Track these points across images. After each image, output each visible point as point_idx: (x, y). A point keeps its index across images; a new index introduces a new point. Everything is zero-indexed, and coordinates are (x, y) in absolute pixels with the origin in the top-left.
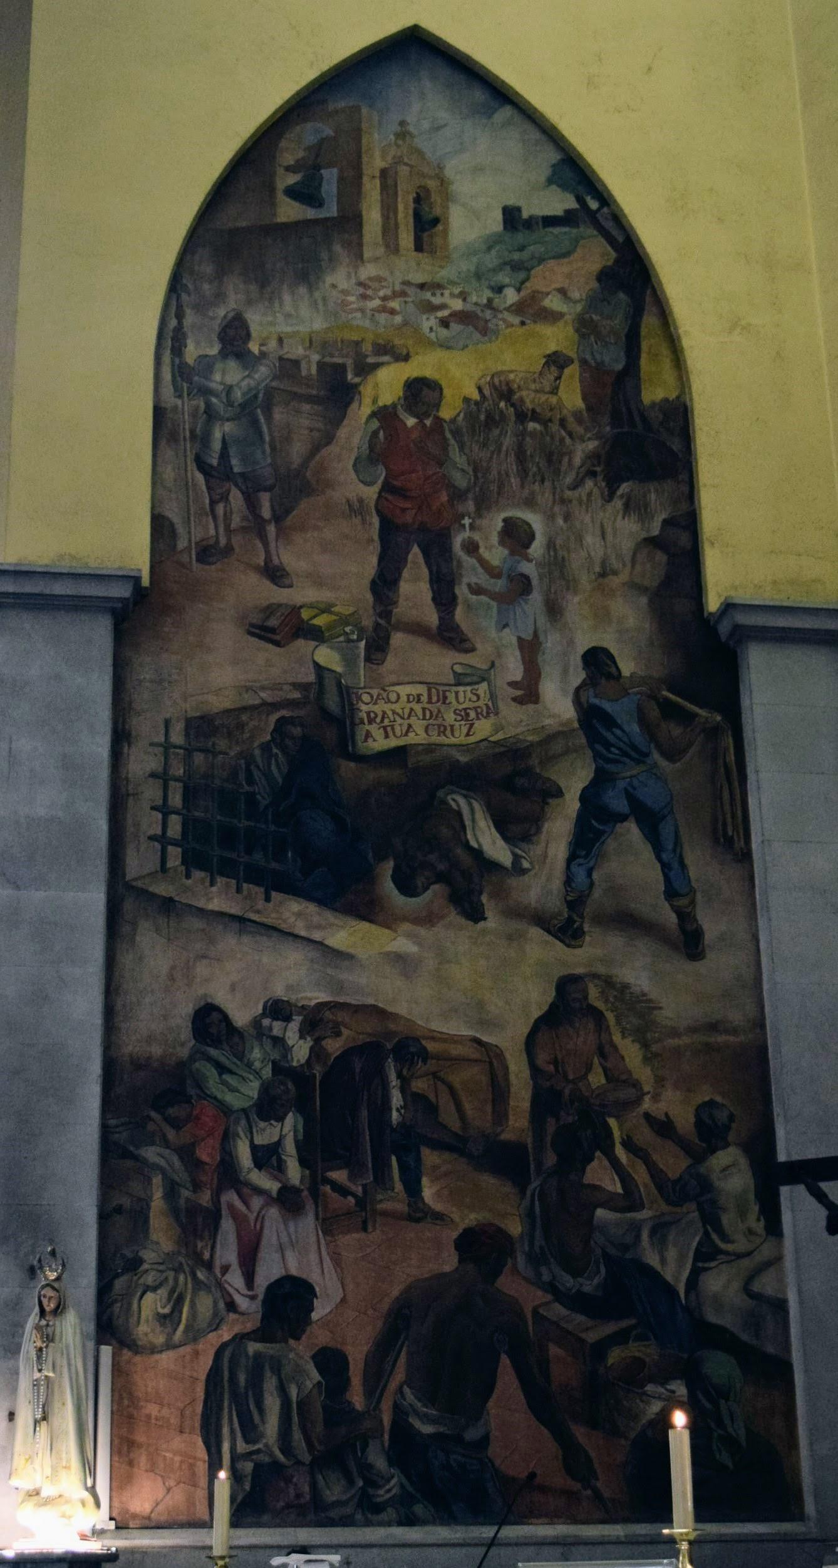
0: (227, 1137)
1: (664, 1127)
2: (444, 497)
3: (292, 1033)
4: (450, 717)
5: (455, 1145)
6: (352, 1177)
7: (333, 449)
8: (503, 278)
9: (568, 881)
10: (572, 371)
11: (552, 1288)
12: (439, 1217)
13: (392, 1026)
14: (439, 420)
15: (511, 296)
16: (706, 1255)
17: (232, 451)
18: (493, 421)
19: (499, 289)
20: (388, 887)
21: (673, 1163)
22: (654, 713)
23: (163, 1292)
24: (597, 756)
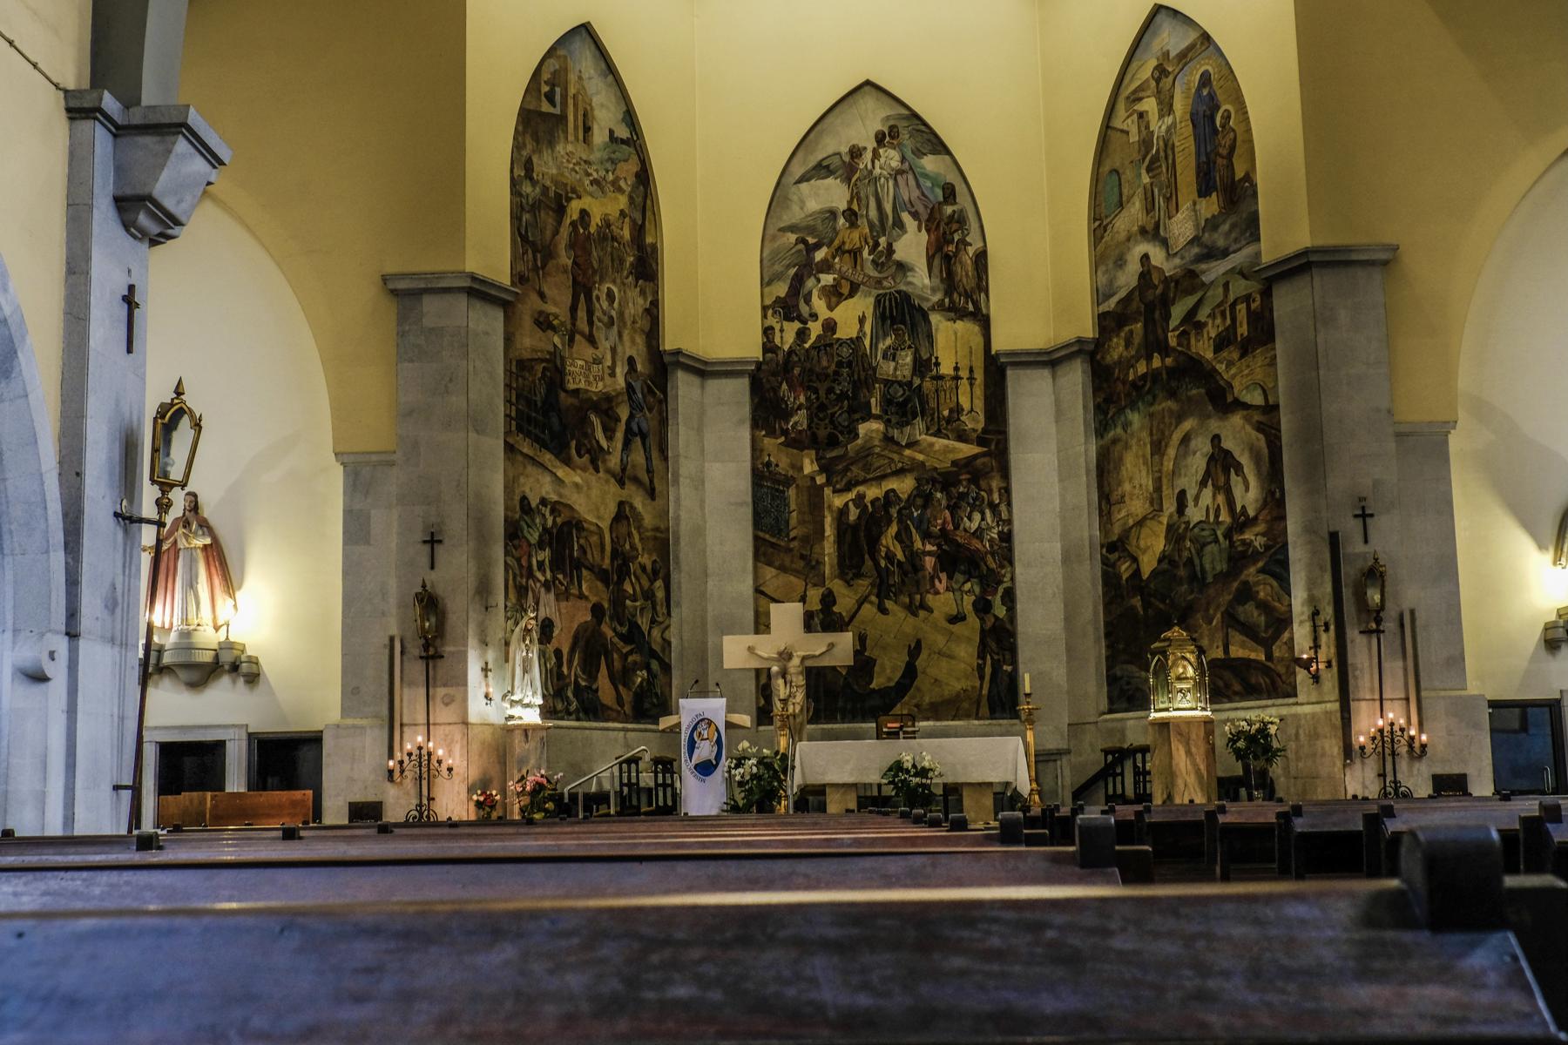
0: (530, 556)
1: (643, 568)
2: (590, 272)
4: (592, 379)
5: (591, 569)
6: (564, 578)
7: (557, 237)
8: (609, 165)
9: (622, 460)
10: (627, 220)
11: (614, 630)
12: (586, 598)
13: (576, 516)
14: (589, 232)
15: (611, 177)
16: (653, 621)
19: (607, 171)
21: (646, 583)
22: (646, 390)
23: (513, 620)
24: (631, 406)
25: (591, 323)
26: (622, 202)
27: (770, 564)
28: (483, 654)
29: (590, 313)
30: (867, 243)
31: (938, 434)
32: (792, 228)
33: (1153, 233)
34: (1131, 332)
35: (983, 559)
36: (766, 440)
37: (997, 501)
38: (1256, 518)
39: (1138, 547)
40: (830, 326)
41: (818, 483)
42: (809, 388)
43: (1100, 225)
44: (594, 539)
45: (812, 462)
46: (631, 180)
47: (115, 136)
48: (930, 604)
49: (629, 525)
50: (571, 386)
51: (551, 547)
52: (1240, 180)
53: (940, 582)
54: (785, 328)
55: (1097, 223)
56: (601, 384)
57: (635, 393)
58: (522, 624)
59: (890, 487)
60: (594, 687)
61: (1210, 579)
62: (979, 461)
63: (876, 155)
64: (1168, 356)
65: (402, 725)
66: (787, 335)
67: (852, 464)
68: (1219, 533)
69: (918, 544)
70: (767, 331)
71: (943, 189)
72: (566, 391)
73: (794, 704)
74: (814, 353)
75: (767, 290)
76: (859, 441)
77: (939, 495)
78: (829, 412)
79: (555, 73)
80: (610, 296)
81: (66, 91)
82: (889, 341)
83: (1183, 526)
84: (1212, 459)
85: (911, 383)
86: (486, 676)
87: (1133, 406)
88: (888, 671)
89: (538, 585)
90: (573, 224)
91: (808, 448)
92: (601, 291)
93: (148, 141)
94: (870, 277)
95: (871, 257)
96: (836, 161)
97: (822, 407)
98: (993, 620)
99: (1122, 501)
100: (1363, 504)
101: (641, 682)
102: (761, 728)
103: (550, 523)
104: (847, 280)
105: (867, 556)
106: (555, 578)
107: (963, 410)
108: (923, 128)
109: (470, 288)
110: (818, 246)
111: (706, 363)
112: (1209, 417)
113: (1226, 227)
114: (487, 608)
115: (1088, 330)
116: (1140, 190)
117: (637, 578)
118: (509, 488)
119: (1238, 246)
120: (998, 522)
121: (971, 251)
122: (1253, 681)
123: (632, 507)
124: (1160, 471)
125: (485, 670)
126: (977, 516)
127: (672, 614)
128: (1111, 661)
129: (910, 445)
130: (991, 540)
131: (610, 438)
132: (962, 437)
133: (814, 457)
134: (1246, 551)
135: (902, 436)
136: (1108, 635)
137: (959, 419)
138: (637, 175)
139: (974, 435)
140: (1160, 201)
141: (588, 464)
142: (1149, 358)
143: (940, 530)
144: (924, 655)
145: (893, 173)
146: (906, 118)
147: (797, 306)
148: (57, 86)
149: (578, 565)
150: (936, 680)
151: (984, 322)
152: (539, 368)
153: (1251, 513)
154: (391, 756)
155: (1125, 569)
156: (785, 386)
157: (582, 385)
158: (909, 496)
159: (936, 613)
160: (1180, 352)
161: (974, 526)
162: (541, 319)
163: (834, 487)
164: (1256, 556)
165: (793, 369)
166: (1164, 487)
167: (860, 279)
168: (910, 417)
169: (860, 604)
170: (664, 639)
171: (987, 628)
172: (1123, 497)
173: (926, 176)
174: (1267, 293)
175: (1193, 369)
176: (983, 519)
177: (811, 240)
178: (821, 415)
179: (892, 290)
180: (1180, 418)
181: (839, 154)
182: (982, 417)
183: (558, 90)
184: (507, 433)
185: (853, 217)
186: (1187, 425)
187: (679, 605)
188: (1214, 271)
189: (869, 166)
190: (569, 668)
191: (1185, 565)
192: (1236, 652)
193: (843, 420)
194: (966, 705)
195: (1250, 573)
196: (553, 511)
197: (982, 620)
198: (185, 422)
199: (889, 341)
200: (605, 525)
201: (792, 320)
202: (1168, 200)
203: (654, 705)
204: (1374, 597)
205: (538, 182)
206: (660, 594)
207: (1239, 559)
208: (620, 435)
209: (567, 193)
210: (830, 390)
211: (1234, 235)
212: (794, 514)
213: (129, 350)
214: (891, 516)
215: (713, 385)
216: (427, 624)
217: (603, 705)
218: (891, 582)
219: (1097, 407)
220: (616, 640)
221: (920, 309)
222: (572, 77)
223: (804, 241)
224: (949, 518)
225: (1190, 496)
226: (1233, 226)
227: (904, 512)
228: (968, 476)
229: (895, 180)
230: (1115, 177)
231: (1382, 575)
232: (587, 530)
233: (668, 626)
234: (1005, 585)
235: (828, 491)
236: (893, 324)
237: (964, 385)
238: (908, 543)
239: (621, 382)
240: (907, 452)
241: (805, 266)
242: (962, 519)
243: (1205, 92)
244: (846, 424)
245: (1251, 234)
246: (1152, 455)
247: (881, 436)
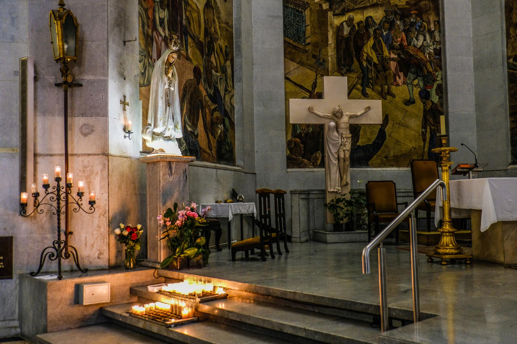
16: (226, 90)
27: (293, 60)
28: (122, 87)
35: (425, 65)
37: (433, 29)
41: (324, 8)
44: (195, 15)
48: (394, 93)
51: (168, 10)
53: (400, 78)
58: (165, 56)
59: (369, 15)
60: (196, 133)
65: (35, 155)
69: (386, 53)
73: (344, 151)
77: (398, 22)
86: (124, 110)
88: (368, 134)
89: (160, 38)
98: (431, 104)
102: (289, 170)
105: (355, 59)
114: (125, 43)
117: (218, 55)
120: (433, 42)
125: (124, 103)
126: (421, 38)
127: (235, 88)
130: (429, 54)
143: (399, 45)
144: (390, 125)
150: (397, 141)
154: (23, 188)
158: (381, 21)
161: (420, 44)
163: (334, 12)
171: (428, 109)
176: (425, 40)
187: (240, 80)
197: (424, 103)
212: (309, 28)
214: (370, 34)
216: (66, 47)
217: (201, 148)
218: (370, 76)
220: (207, 99)
224: (405, 38)
227: (377, 31)
228: (416, 12)
232: (191, 7)
234: (438, 82)
235: (330, 14)
238: (380, 52)
242: (412, 39)
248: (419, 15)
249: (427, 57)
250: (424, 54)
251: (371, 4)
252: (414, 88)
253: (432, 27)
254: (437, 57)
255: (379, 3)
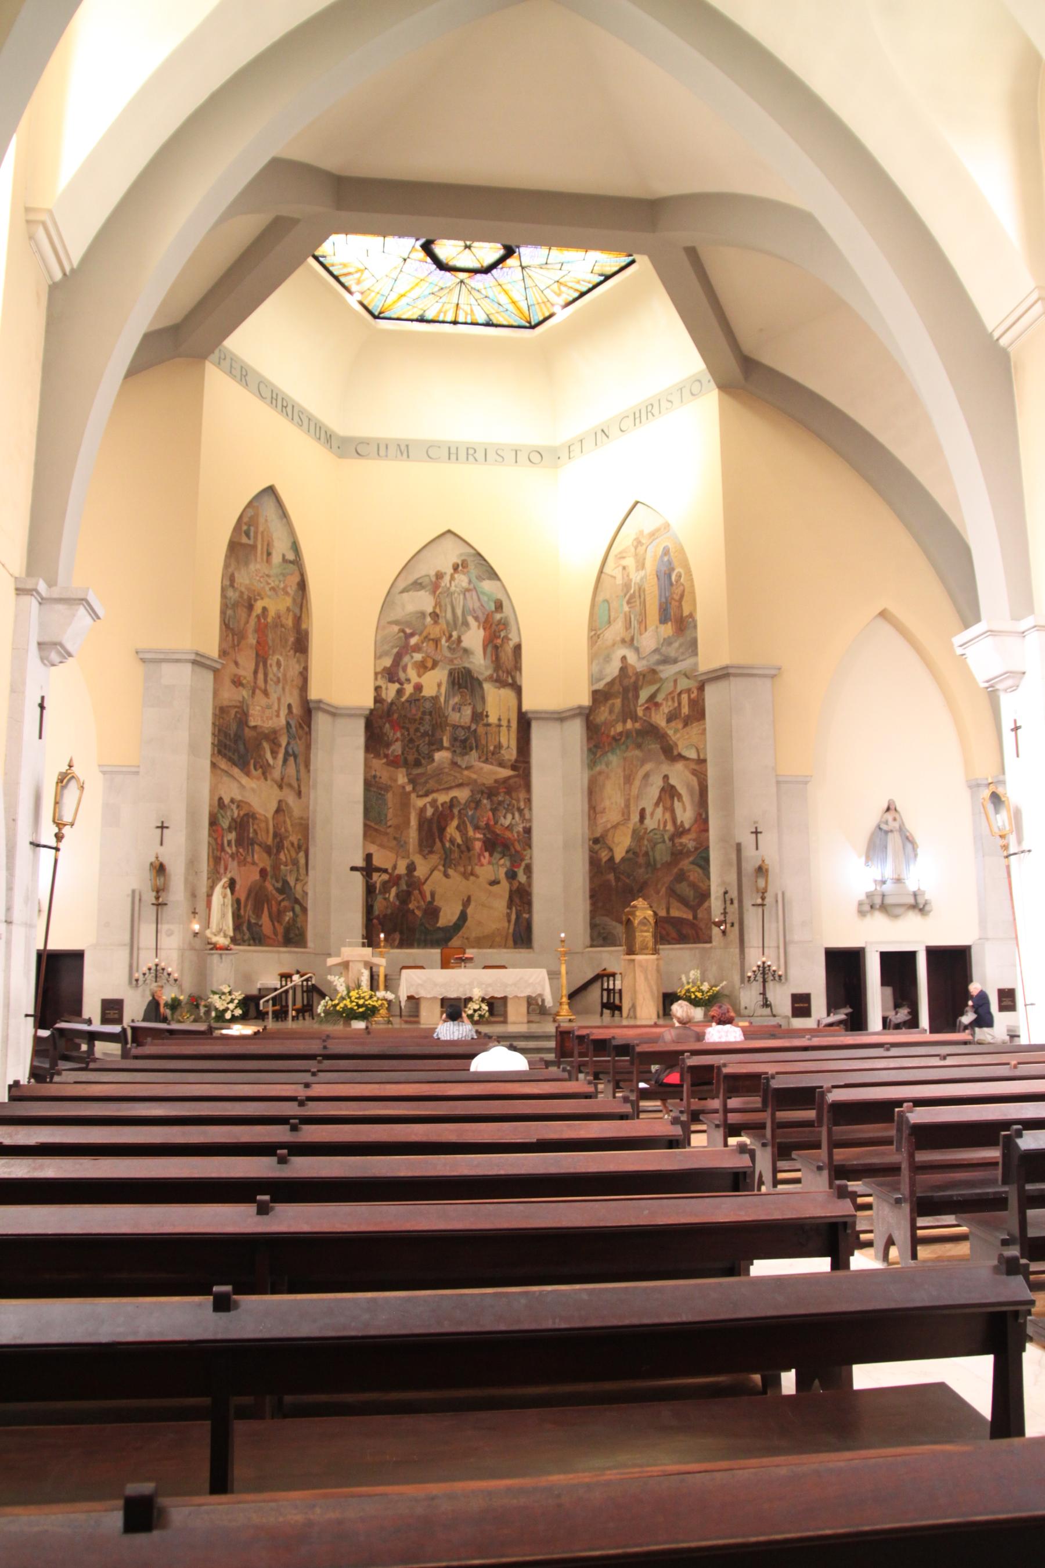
0: (223, 837)
1: (292, 844)
3: (234, 807)
4: (265, 719)
6: (244, 851)
7: (248, 625)
8: (281, 578)
9: (281, 772)
11: (274, 886)
15: (282, 585)
16: (297, 880)
17: (231, 620)
18: (276, 626)
20: (252, 767)
21: (293, 854)
22: (298, 726)
25: (266, 681)
26: (288, 602)
29: (266, 675)
30: (444, 634)
31: (486, 761)
32: (396, 622)
33: (630, 642)
34: (613, 704)
35: (513, 845)
36: (374, 761)
38: (689, 830)
39: (613, 842)
40: (418, 688)
42: (403, 728)
43: (595, 634)
44: (263, 825)
45: (404, 776)
46: (294, 587)
47: (40, 604)
49: (284, 815)
50: (252, 724)
52: (687, 616)
53: (484, 857)
54: (389, 687)
55: (593, 633)
56: (270, 722)
57: (291, 727)
61: (659, 866)
62: (512, 781)
63: (452, 578)
64: (636, 721)
66: (390, 692)
67: (429, 779)
68: (666, 837)
70: (377, 689)
71: (495, 603)
72: (249, 727)
74: (407, 705)
75: (378, 661)
76: (435, 764)
77: (485, 801)
78: (416, 744)
79: (251, 518)
80: (279, 664)
81: (16, 578)
82: (457, 699)
83: (643, 831)
84: (663, 790)
85: (469, 728)
87: (613, 751)
89: (227, 856)
90: (258, 617)
91: (401, 767)
92: (272, 661)
93: (60, 607)
94: (446, 657)
95: (447, 644)
96: (426, 581)
97: (411, 741)
98: (517, 884)
99: (603, 811)
100: (756, 825)
101: (289, 920)
103: (236, 815)
104: (431, 658)
105: (437, 840)
106: (238, 851)
107: (502, 747)
108: (483, 562)
109: (194, 660)
110: (412, 635)
111: (337, 708)
112: (662, 763)
113: (676, 645)
115: (585, 700)
116: (622, 616)
117: (288, 851)
118: (213, 790)
119: (684, 657)
121: (512, 644)
122: (684, 932)
123: (287, 804)
124: (629, 794)
126: (509, 816)
128: (594, 913)
129: (468, 768)
130: (518, 832)
131: (275, 758)
132: (501, 764)
133: (405, 773)
134: (682, 850)
135: (463, 762)
136: (592, 897)
137: (500, 753)
138: (298, 584)
139: (510, 764)
140: (635, 623)
141: (261, 775)
142: (625, 722)
143: (486, 824)
145: (463, 590)
146: (474, 555)
147: (397, 673)
148: (11, 575)
149: (252, 842)
151: (518, 690)
152: (233, 712)
153: (687, 826)
155: (604, 855)
156: (387, 725)
157: (259, 723)
159: (481, 879)
160: (645, 721)
161: (507, 822)
162: (235, 680)
163: (417, 793)
164: (689, 853)
165: (393, 714)
166: (632, 805)
167: (440, 657)
168: (468, 749)
169: (432, 871)
170: (303, 891)
172: (604, 809)
173: (484, 593)
174: (701, 688)
175: (652, 732)
176: (513, 818)
177: (408, 631)
178: (411, 746)
179: (460, 666)
180: (643, 762)
181: (428, 576)
182: (514, 752)
183: (252, 529)
184: (213, 755)
185: (436, 618)
186: (648, 767)
188: (667, 672)
189: (448, 585)
190: (245, 911)
191: (643, 855)
192: (675, 913)
193: (425, 749)
194: (498, 939)
195: (685, 864)
196: (238, 807)
197: (510, 883)
198: (73, 785)
199: (457, 699)
200: (270, 815)
201: (393, 682)
202: (640, 623)
203: (296, 935)
204: (761, 883)
205: (237, 589)
206: (302, 861)
207: (677, 855)
208: (281, 756)
209: (255, 596)
210: (417, 730)
211: (681, 650)
213: (40, 738)
215: (341, 722)
217: (265, 935)
218: (452, 857)
219: (590, 750)
220: (274, 892)
221: (477, 679)
222: (261, 520)
223: (403, 631)
225: (648, 812)
226: (681, 645)
227: (462, 811)
229: (465, 595)
230: (606, 605)
231: (767, 871)
233: (306, 883)
234: (527, 862)
235: (413, 796)
236: (460, 688)
237: (504, 729)
239: (282, 721)
240: (466, 773)
241: (404, 647)
243: (666, 559)
244: (426, 752)
245: (692, 651)
246: (625, 784)
247: (449, 761)
248: (509, 791)
249: (516, 835)
250: (512, 833)
251: (457, 783)
252: (500, 868)
253: (522, 805)
254: (526, 835)
255: (465, 782)
